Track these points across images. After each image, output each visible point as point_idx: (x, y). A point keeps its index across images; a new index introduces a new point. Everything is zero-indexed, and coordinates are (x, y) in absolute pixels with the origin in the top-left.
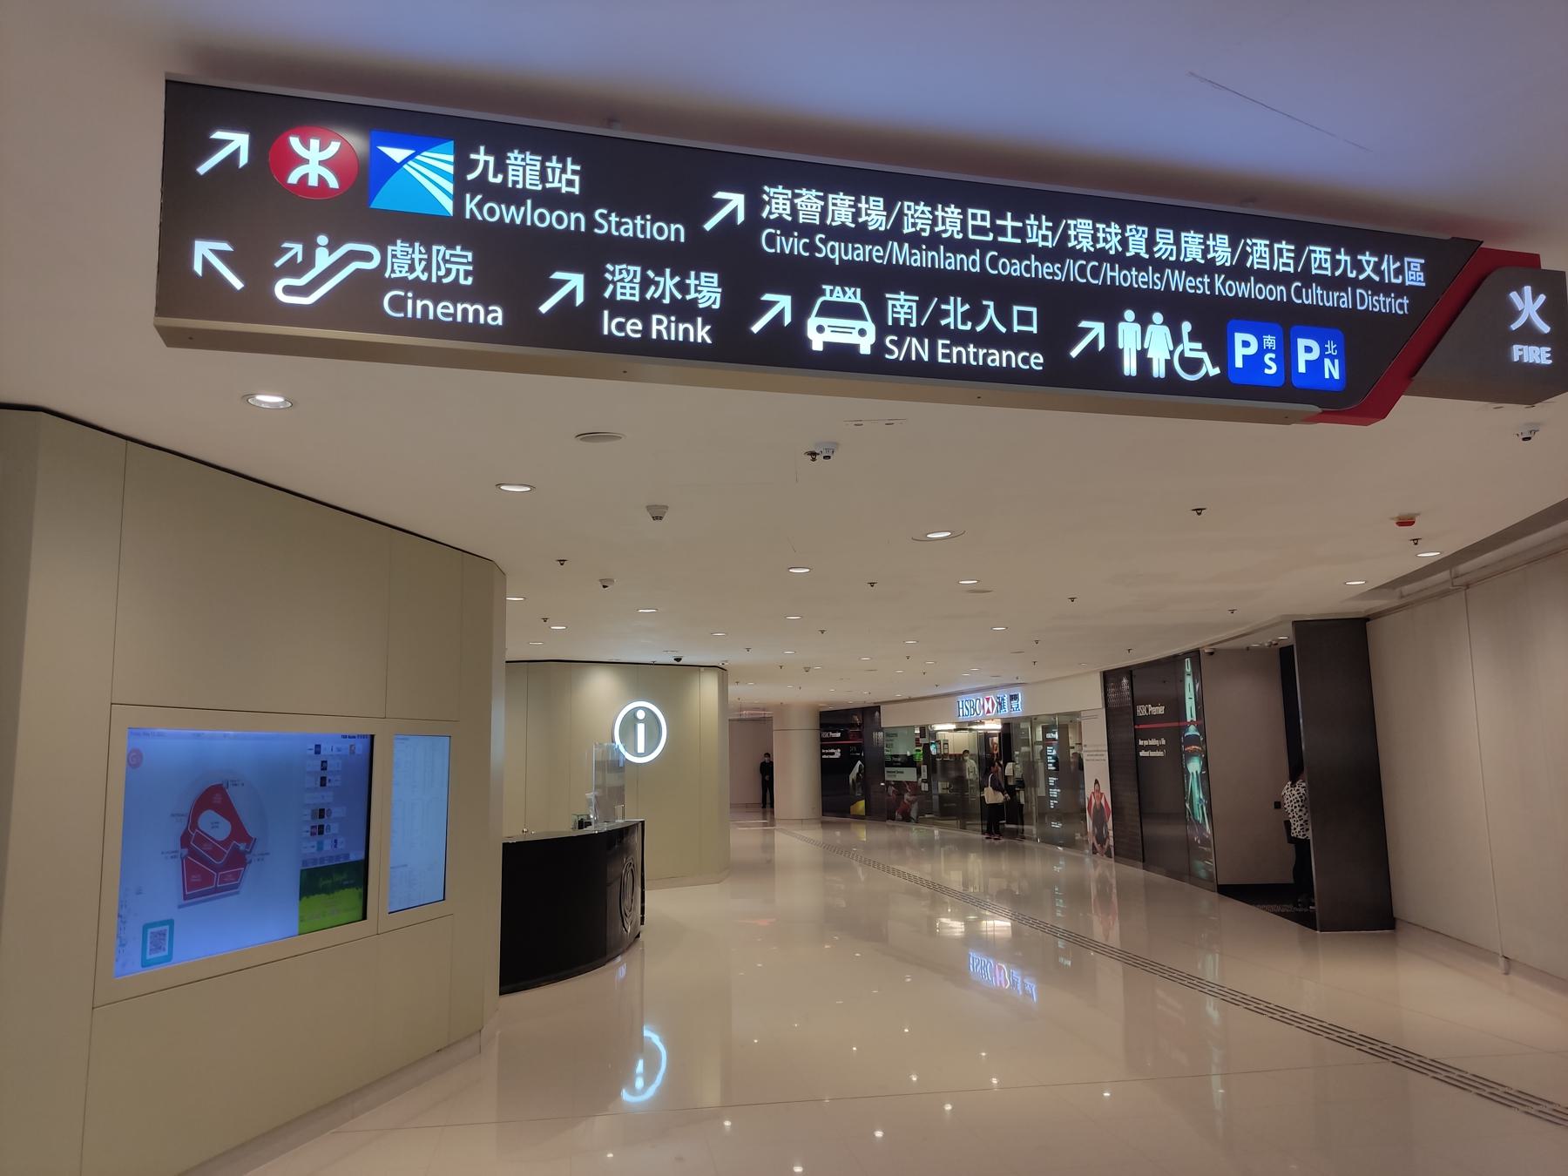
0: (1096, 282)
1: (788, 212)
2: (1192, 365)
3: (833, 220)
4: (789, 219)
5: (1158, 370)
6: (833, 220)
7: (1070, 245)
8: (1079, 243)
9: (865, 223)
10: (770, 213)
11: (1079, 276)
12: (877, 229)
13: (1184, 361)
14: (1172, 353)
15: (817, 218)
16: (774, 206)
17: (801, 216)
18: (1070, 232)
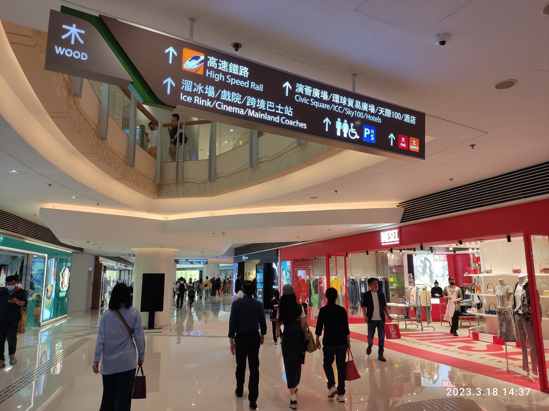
0: (341, 112)
1: (303, 91)
2: (353, 135)
3: (314, 95)
4: (303, 93)
5: (345, 135)
6: (314, 95)
7: (333, 101)
8: (335, 100)
9: (322, 98)
10: (298, 91)
11: (340, 111)
12: (325, 100)
13: (351, 133)
14: (348, 131)
15: (310, 94)
16: (299, 89)
17: (306, 93)
18: (333, 97)
